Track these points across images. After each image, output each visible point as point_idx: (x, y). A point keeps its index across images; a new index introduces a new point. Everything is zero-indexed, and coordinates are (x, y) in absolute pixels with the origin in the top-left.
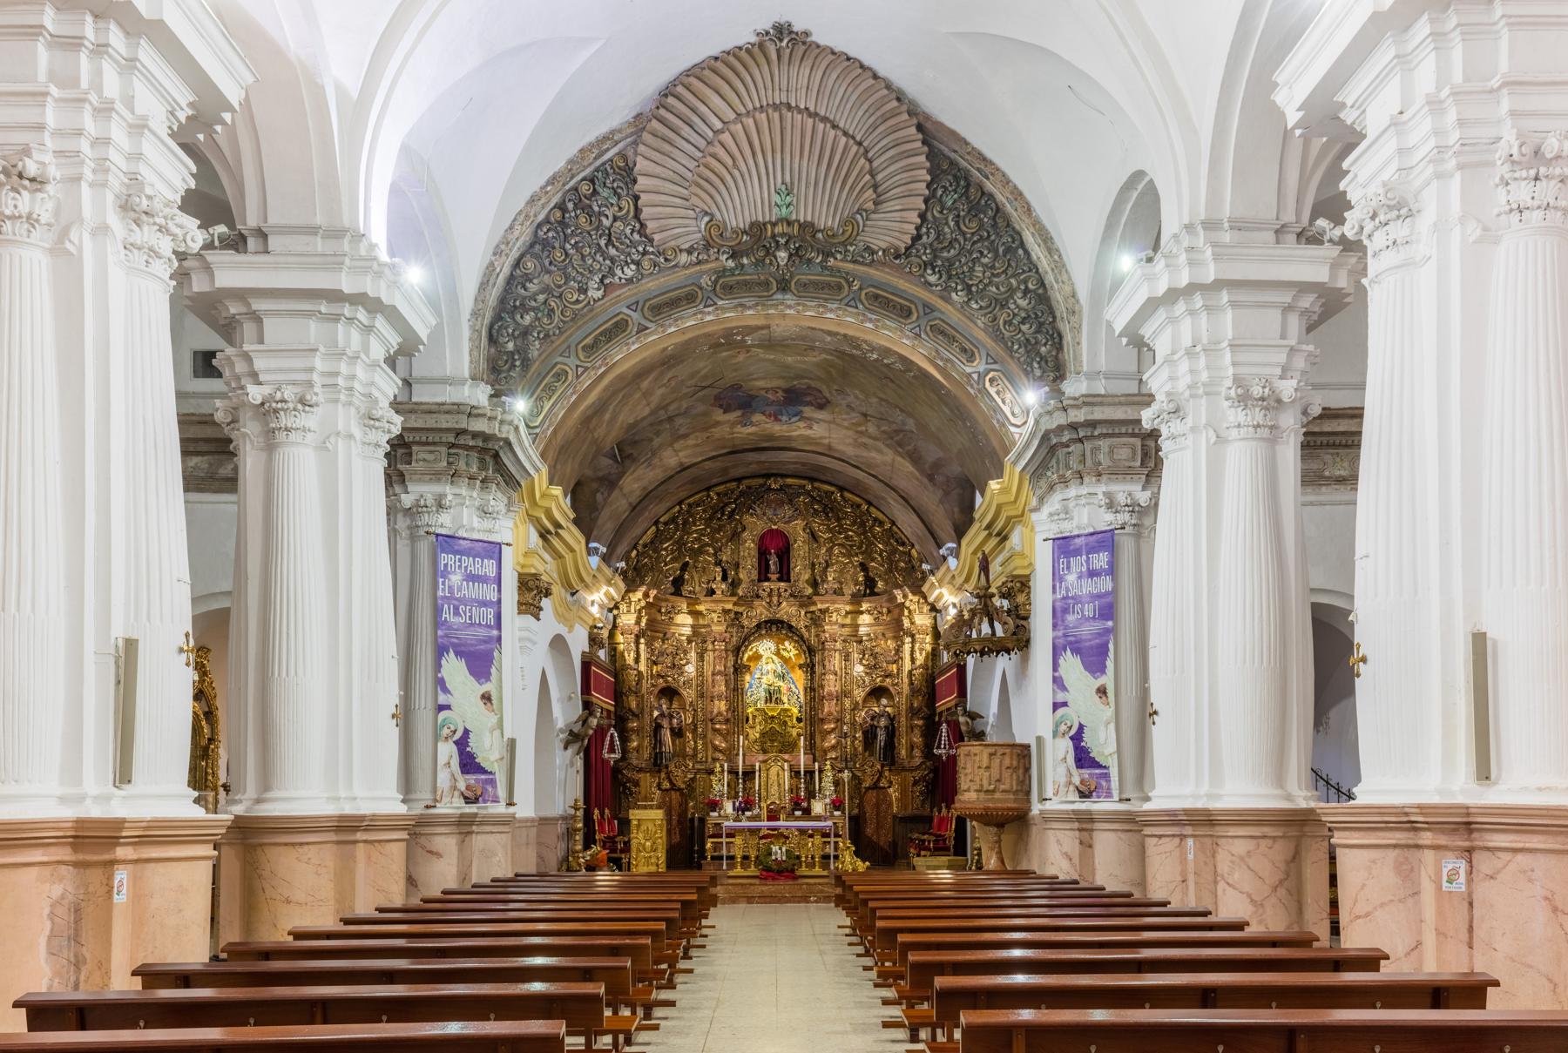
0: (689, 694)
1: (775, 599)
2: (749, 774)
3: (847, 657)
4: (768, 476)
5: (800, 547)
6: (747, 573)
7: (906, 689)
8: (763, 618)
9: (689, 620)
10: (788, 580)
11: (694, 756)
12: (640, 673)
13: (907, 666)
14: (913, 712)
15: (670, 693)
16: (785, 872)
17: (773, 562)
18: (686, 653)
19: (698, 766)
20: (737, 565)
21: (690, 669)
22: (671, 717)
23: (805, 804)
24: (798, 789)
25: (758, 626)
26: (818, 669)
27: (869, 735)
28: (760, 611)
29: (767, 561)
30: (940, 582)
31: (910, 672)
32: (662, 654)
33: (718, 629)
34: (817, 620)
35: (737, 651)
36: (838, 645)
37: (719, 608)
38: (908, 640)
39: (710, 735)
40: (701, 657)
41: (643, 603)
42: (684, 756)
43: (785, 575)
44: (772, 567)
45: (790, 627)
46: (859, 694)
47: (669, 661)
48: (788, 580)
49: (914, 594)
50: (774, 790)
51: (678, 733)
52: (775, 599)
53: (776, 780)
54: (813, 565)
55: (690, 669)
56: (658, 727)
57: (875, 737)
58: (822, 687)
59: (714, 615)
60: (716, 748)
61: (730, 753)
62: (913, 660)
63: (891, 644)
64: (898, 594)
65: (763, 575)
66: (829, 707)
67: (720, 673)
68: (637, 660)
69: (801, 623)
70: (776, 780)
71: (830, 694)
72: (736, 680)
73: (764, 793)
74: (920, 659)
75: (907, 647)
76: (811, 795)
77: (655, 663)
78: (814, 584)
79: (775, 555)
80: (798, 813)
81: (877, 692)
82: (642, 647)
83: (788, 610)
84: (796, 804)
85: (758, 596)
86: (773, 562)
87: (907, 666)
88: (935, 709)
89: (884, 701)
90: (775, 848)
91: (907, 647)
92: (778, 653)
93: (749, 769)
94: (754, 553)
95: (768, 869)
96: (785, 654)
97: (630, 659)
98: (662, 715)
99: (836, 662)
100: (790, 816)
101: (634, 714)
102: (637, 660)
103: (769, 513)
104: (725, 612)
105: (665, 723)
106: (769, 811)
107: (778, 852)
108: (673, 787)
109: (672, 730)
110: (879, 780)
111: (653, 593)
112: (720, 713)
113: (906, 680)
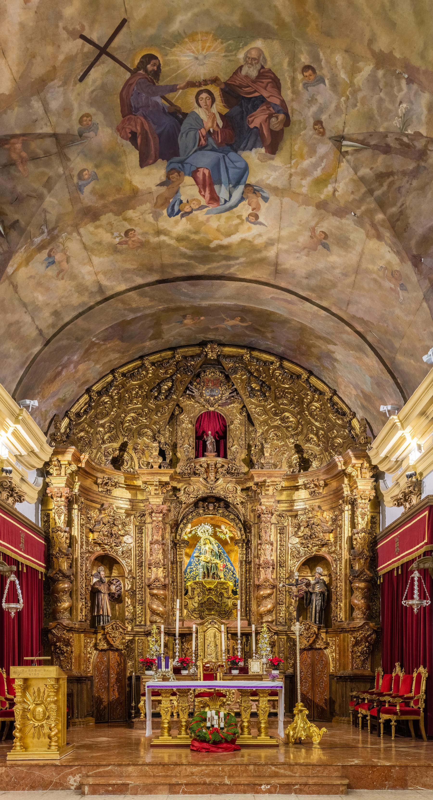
0: (128, 564)
1: (212, 476)
2: (186, 636)
3: (282, 531)
4: (203, 344)
5: (236, 424)
6: (186, 449)
7: (345, 555)
8: (201, 494)
9: (128, 495)
10: (225, 456)
11: (133, 620)
12: (72, 538)
13: (347, 531)
14: (354, 575)
15: (108, 561)
16: (222, 743)
17: (210, 441)
18: (124, 524)
19: (137, 629)
20: (175, 447)
21: (129, 540)
22: (110, 583)
23: (241, 664)
24: (234, 649)
25: (196, 505)
26: (254, 542)
27: (304, 604)
28: (198, 487)
29: (205, 442)
30: (404, 422)
31: (351, 539)
32: (98, 522)
33: (156, 501)
34: (252, 494)
35: (176, 526)
36: (274, 519)
37: (156, 478)
38: (347, 507)
39: (148, 600)
40: (140, 530)
41: (74, 467)
42: (123, 620)
43: (222, 450)
44: (210, 447)
45: (227, 505)
46: (294, 564)
47: (105, 529)
48: (225, 456)
49: (357, 457)
50: (211, 649)
51: (117, 599)
52: (212, 476)
53: (213, 642)
54: (249, 447)
55: (129, 540)
56: (94, 593)
57: (311, 601)
58: (258, 557)
59: (152, 488)
60: (153, 612)
61: (167, 617)
62: (353, 525)
63: (328, 515)
64: (339, 460)
65: (200, 450)
66: (266, 575)
67: (157, 542)
68: (69, 523)
69: (237, 498)
70: (213, 642)
71: (266, 563)
72: (175, 554)
73: (200, 652)
74: (362, 523)
75: (347, 515)
76: (247, 655)
77: (92, 531)
78: (250, 464)
79: (212, 435)
80: (235, 672)
81: (312, 562)
82: (75, 512)
83: (224, 486)
84: (233, 662)
85: (195, 474)
86: (210, 441)
87: (347, 531)
88: (376, 572)
89: (319, 569)
90: (210, 713)
91: (347, 515)
92: (215, 535)
93: (186, 631)
94: (192, 434)
95: (203, 740)
96: (222, 536)
97: (60, 521)
98: (101, 581)
99: (272, 534)
100: (228, 674)
101: (65, 576)
102: (69, 523)
103: (206, 394)
104: (164, 485)
105: (103, 588)
106: (205, 669)
107: (215, 717)
108: (111, 648)
109: (111, 595)
110: (314, 642)
111: (85, 457)
112: (157, 580)
113: (345, 546)
